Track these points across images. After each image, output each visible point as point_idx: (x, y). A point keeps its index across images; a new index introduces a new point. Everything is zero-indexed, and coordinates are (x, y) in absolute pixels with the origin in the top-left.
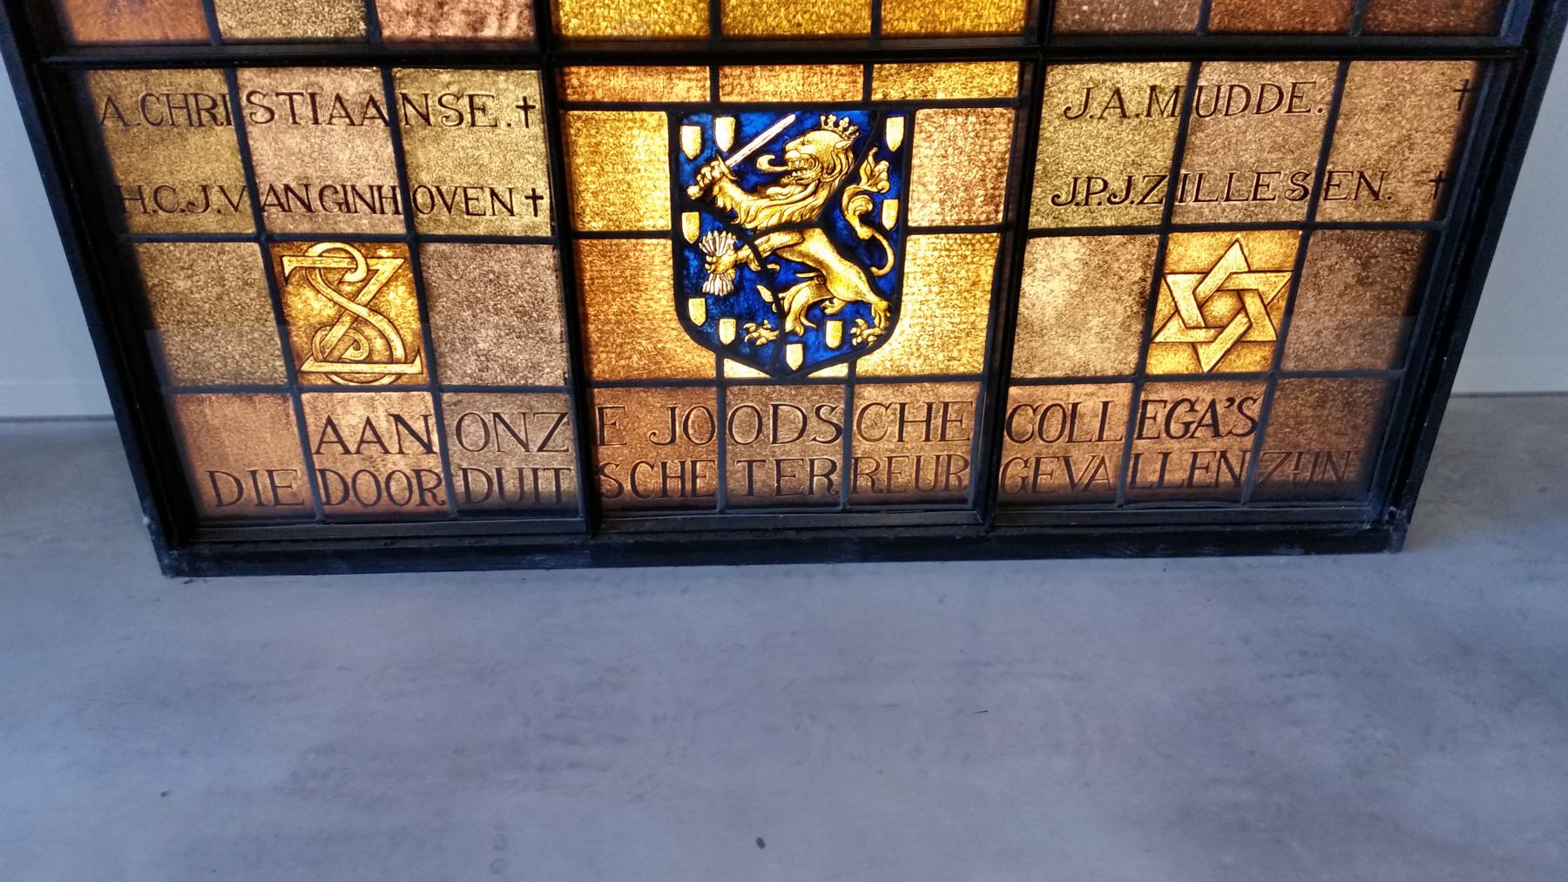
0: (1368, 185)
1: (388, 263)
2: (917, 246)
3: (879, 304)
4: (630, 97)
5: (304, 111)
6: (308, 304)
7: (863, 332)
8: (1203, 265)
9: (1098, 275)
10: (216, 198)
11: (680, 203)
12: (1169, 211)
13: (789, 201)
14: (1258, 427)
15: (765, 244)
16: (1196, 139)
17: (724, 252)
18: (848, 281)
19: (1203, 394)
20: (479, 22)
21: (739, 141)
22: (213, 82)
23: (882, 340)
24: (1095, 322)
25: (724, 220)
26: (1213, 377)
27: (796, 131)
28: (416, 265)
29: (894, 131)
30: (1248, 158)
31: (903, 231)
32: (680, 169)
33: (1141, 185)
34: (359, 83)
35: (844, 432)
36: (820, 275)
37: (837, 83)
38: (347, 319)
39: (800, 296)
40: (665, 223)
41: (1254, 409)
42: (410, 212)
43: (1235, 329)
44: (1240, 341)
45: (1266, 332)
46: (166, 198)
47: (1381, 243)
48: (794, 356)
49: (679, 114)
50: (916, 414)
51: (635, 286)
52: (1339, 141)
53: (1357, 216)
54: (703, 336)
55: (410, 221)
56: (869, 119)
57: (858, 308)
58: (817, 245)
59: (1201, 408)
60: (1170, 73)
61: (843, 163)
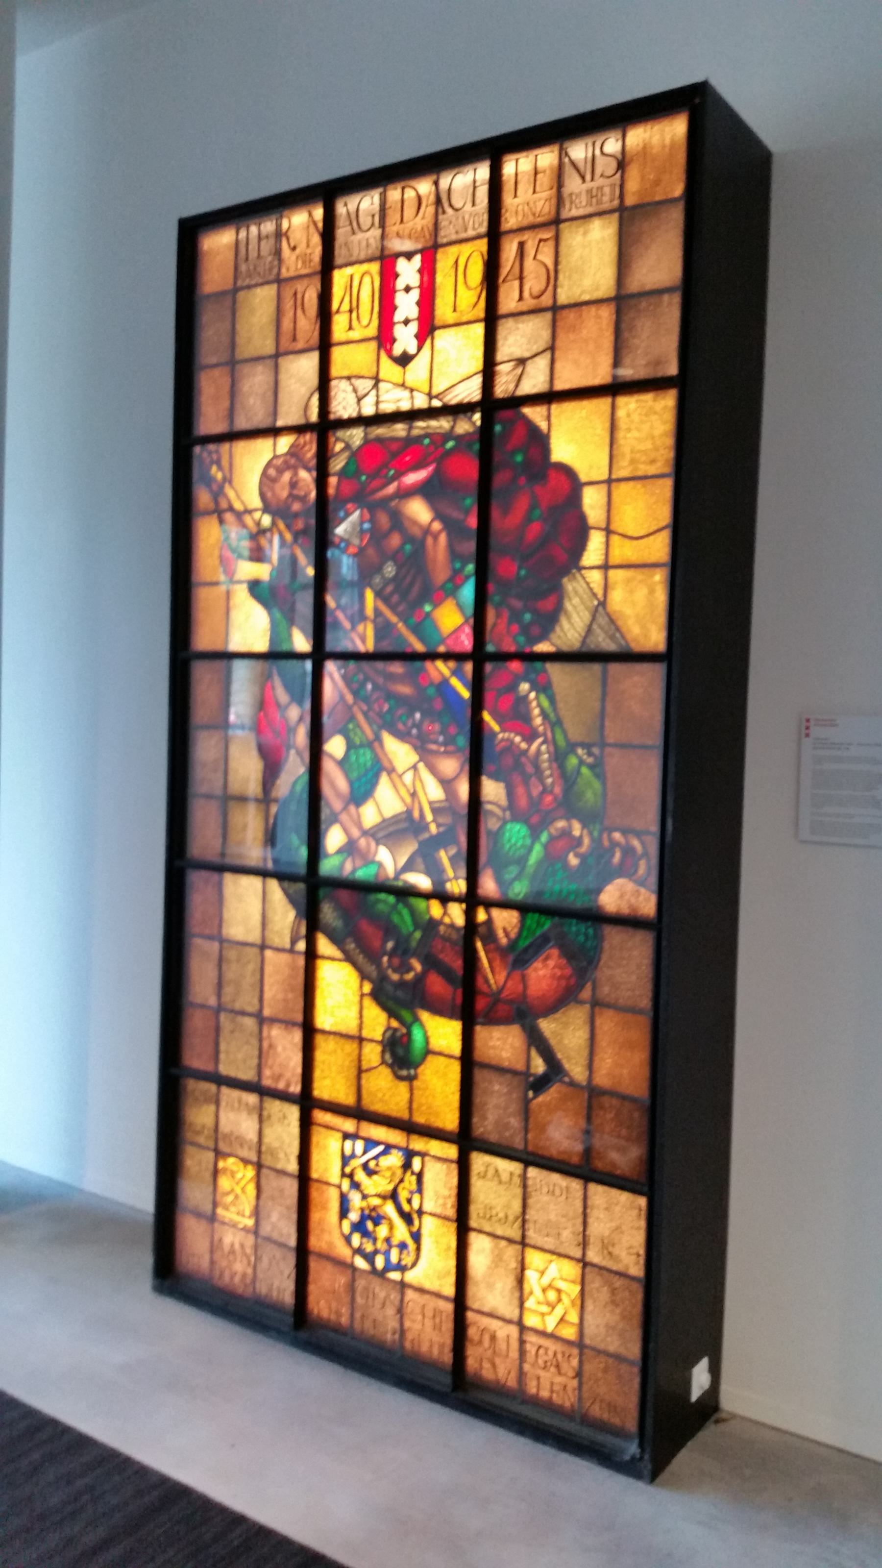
0: (606, 1246)
1: (250, 1172)
2: (426, 1219)
3: (412, 1245)
4: (331, 1125)
5: (236, 1105)
7: (407, 1260)
8: (541, 1268)
9: (497, 1260)
12: (524, 1236)
14: (579, 1374)
16: (530, 1201)
17: (355, 1199)
18: (401, 1232)
19: (552, 1346)
20: (288, 1085)
21: (365, 1152)
22: (213, 1087)
23: (414, 1265)
24: (499, 1286)
25: (356, 1185)
26: (552, 1336)
27: (384, 1153)
28: (258, 1176)
29: (417, 1163)
30: (552, 1217)
31: (420, 1212)
32: (345, 1160)
33: (511, 1218)
34: (252, 1099)
36: (391, 1227)
37: (395, 1137)
39: (382, 1231)
41: (575, 1362)
42: (259, 1152)
43: (559, 1311)
44: (562, 1320)
45: (573, 1317)
47: (618, 1282)
48: (380, 1262)
49: (346, 1136)
50: (429, 1313)
51: (325, 1207)
52: (590, 1220)
53: (604, 1263)
54: (348, 1239)
55: (259, 1157)
56: (409, 1155)
57: (403, 1246)
58: (389, 1209)
59: (551, 1353)
60: (515, 1167)
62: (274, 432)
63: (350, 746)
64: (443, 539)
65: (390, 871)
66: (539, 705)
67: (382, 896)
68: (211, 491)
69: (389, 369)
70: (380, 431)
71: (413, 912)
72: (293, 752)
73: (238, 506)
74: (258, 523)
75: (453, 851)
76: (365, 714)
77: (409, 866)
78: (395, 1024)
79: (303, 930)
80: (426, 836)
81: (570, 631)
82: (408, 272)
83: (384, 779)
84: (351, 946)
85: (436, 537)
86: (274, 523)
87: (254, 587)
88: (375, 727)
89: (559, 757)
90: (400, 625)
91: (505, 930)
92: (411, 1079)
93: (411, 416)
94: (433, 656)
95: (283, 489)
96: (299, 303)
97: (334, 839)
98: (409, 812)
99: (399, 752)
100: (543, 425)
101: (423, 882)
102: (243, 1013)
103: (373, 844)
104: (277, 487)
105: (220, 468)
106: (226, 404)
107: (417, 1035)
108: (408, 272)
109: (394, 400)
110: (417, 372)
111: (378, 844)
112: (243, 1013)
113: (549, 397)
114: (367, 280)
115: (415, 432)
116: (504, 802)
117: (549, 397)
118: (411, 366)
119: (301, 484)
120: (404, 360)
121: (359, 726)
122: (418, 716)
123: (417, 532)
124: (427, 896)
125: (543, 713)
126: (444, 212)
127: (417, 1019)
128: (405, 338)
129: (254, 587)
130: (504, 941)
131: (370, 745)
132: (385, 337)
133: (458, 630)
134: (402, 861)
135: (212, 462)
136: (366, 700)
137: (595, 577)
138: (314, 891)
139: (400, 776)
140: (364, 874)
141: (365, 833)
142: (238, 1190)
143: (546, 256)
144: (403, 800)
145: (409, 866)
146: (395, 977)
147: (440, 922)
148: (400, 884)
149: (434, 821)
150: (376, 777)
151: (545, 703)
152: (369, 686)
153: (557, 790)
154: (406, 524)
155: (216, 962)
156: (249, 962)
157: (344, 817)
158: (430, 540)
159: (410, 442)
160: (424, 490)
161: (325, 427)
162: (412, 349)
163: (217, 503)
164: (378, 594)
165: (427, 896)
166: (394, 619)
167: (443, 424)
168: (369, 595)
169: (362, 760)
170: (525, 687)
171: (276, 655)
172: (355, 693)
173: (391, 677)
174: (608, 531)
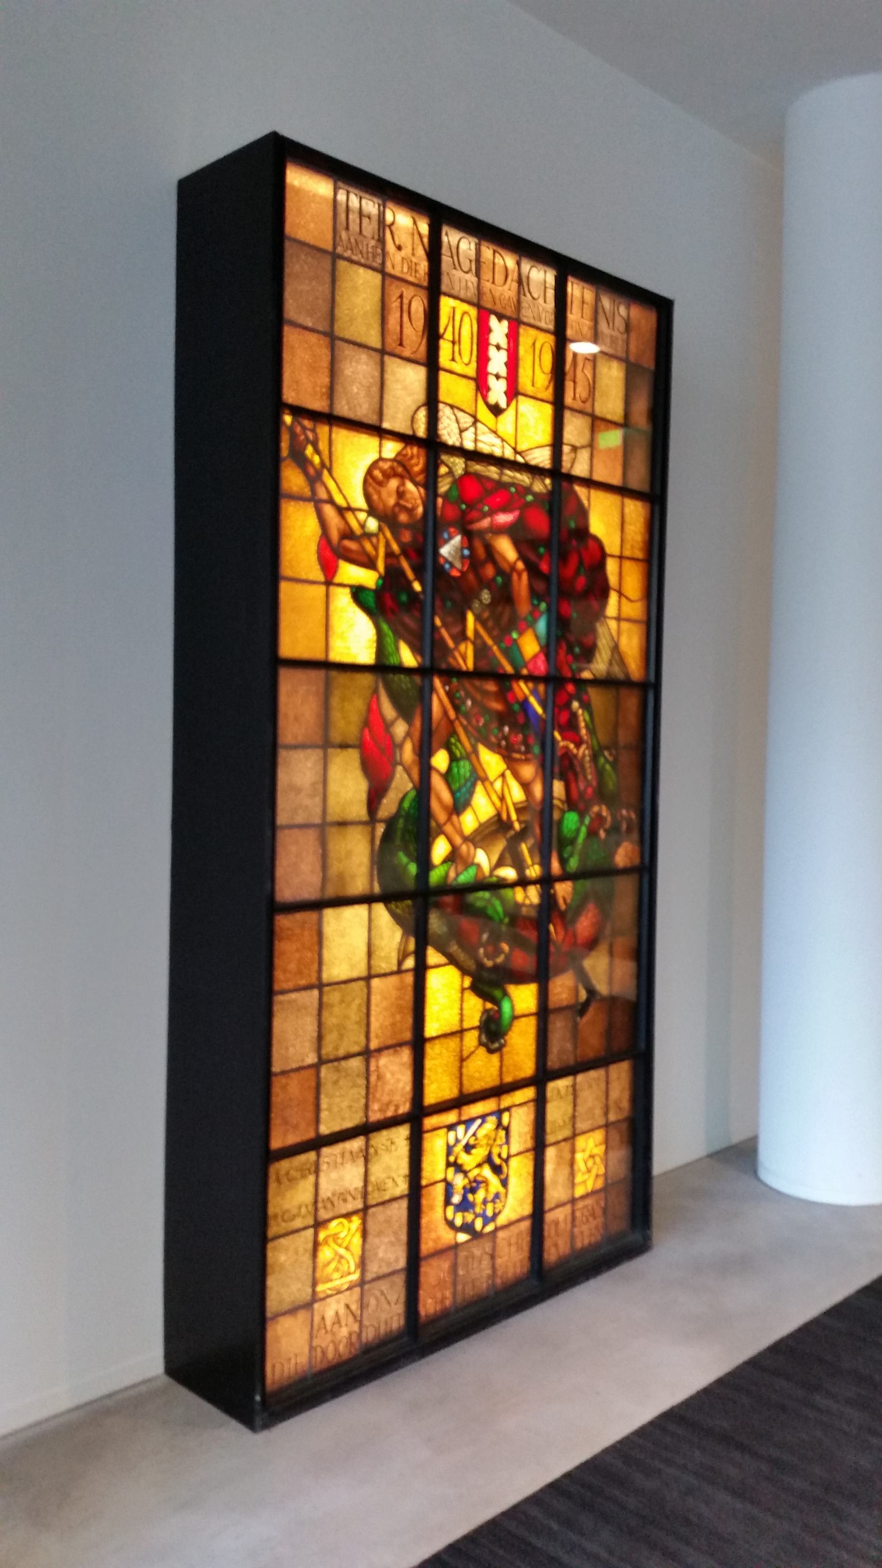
4: (437, 1126)
6: (325, 1254)
10: (303, 1210)
11: (448, 1164)
13: (479, 1153)
15: (471, 1175)
17: (459, 1182)
25: (459, 1168)
32: (449, 1150)
35: (493, 1257)
38: (337, 1258)
40: (441, 1176)
46: (286, 1217)
51: (432, 1208)
58: (487, 1171)
61: (493, 1135)
62: (378, 431)
63: (453, 758)
64: (525, 576)
65: (486, 868)
66: (584, 720)
67: (481, 894)
68: (306, 473)
69: (484, 413)
70: (478, 468)
71: (503, 901)
72: (399, 769)
73: (339, 500)
74: (363, 526)
75: (531, 841)
76: (465, 728)
77: (500, 863)
78: (489, 1005)
79: (412, 946)
80: (512, 833)
81: (600, 665)
82: (499, 330)
83: (479, 789)
84: (454, 948)
85: (520, 575)
86: (380, 529)
87: (358, 593)
88: (473, 741)
89: (595, 757)
90: (495, 648)
91: (565, 900)
92: (499, 1050)
93: (501, 462)
94: (517, 676)
95: (390, 495)
96: (405, 309)
97: (440, 849)
98: (499, 815)
99: (491, 762)
100: (585, 502)
101: (509, 873)
102: (348, 1057)
103: (472, 848)
104: (384, 491)
105: (317, 451)
106: (326, 380)
107: (506, 1007)
108: (499, 330)
109: (489, 444)
110: (505, 423)
111: (476, 847)
112: (348, 1057)
113: (589, 483)
114: (466, 319)
115: (505, 479)
116: (563, 797)
117: (589, 483)
118: (501, 418)
119: (408, 496)
120: (496, 410)
121: (459, 740)
122: (506, 729)
123: (507, 568)
124: (513, 885)
125: (587, 726)
126: (525, 295)
127: (506, 994)
128: (498, 391)
129: (358, 593)
130: (563, 907)
131: (468, 757)
132: (481, 383)
133: (535, 657)
134: (495, 858)
135: (308, 441)
136: (467, 716)
137: (613, 624)
138: (422, 904)
139: (492, 784)
140: (466, 877)
141: (466, 839)
142: (342, 1251)
143: (589, 373)
144: (494, 804)
145: (500, 863)
146: (489, 963)
147: (523, 905)
148: (494, 879)
149: (518, 820)
150: (474, 785)
151: (587, 718)
152: (469, 703)
153: (594, 783)
154: (497, 557)
155: (315, 1012)
156: (353, 1000)
157: (448, 828)
158: (515, 577)
159: (501, 486)
160: (508, 530)
161: (433, 446)
162: (503, 404)
163: (313, 491)
164: (478, 618)
165: (513, 885)
166: (490, 642)
167: (524, 478)
168: (470, 618)
169: (462, 771)
170: (575, 704)
171: (383, 667)
172: (456, 708)
173: (486, 693)
174: (620, 594)
